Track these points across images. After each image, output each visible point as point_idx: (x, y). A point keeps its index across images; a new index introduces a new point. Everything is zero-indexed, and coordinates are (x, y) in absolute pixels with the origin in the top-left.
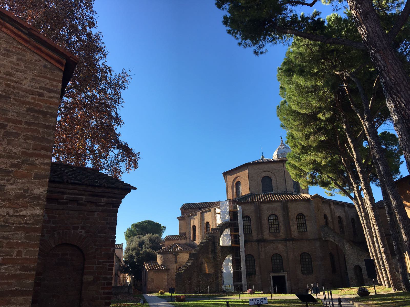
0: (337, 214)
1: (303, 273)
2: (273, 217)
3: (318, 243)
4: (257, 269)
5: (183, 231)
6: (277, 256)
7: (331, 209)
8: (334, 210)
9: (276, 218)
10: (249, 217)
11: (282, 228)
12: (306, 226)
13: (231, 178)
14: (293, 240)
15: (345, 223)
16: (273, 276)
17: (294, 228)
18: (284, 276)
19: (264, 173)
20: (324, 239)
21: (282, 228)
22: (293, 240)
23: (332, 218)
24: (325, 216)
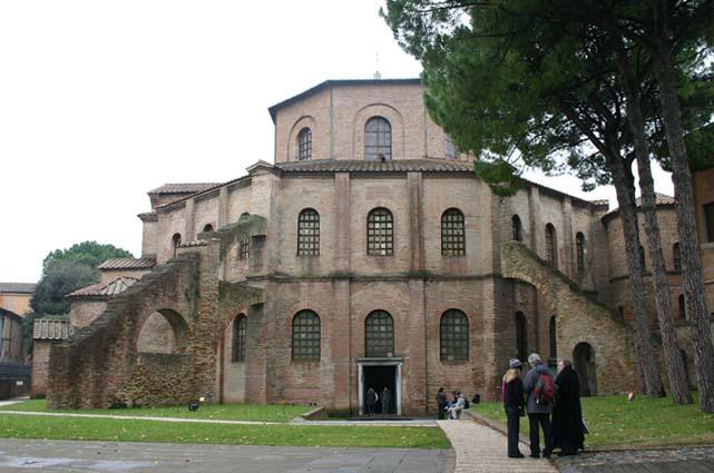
0: (545, 219)
1: (443, 357)
2: (380, 216)
3: (489, 286)
4: (326, 348)
5: (150, 251)
6: (378, 316)
7: (531, 202)
8: (539, 208)
9: (389, 218)
10: (316, 213)
11: (402, 242)
12: (464, 242)
13: (288, 119)
14: (425, 277)
15: (560, 243)
16: (365, 368)
17: (433, 245)
18: (395, 367)
19: (373, 108)
20: (505, 276)
21: (402, 242)
22: (425, 277)
23: (533, 224)
24: (516, 219)
